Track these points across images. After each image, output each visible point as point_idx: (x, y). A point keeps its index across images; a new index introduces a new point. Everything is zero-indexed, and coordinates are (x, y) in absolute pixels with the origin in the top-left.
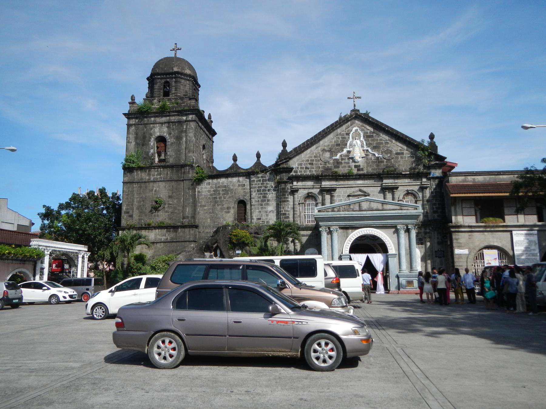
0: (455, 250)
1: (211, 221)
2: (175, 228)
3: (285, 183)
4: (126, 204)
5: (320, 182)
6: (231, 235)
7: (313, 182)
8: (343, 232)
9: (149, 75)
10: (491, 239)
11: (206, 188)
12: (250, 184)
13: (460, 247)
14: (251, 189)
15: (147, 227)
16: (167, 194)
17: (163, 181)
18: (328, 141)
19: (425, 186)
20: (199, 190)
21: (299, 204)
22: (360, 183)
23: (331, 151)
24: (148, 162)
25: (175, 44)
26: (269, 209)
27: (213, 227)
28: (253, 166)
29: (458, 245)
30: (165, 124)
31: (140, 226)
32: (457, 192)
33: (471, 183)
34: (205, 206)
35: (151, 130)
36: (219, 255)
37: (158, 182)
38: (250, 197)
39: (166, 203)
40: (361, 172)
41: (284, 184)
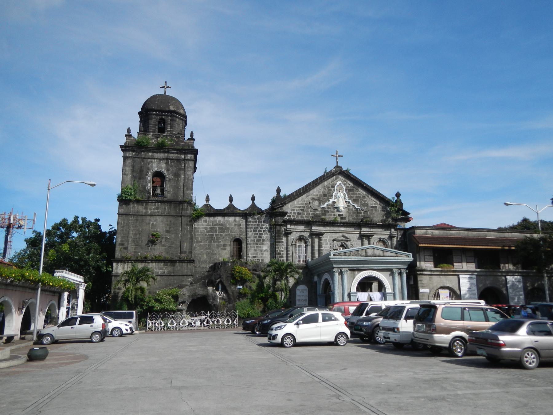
0: (420, 289)
1: (207, 257)
2: (172, 262)
3: (280, 225)
4: (121, 236)
5: (310, 226)
6: (233, 271)
7: (304, 227)
8: (351, 274)
9: (140, 110)
11: (203, 225)
12: (246, 224)
13: (423, 287)
14: (248, 229)
15: (143, 261)
16: (165, 228)
17: (161, 215)
18: (317, 191)
19: (394, 235)
20: (195, 226)
21: (292, 245)
22: (343, 230)
24: (145, 196)
25: (166, 82)
26: (264, 248)
27: (210, 262)
28: (250, 207)
29: (422, 285)
30: (163, 160)
31: (135, 258)
32: (428, 243)
33: (430, 236)
34: (201, 242)
35: (148, 165)
36: (220, 289)
37: (155, 217)
38: (245, 237)
39: (163, 237)
40: (344, 221)
41: (279, 227)
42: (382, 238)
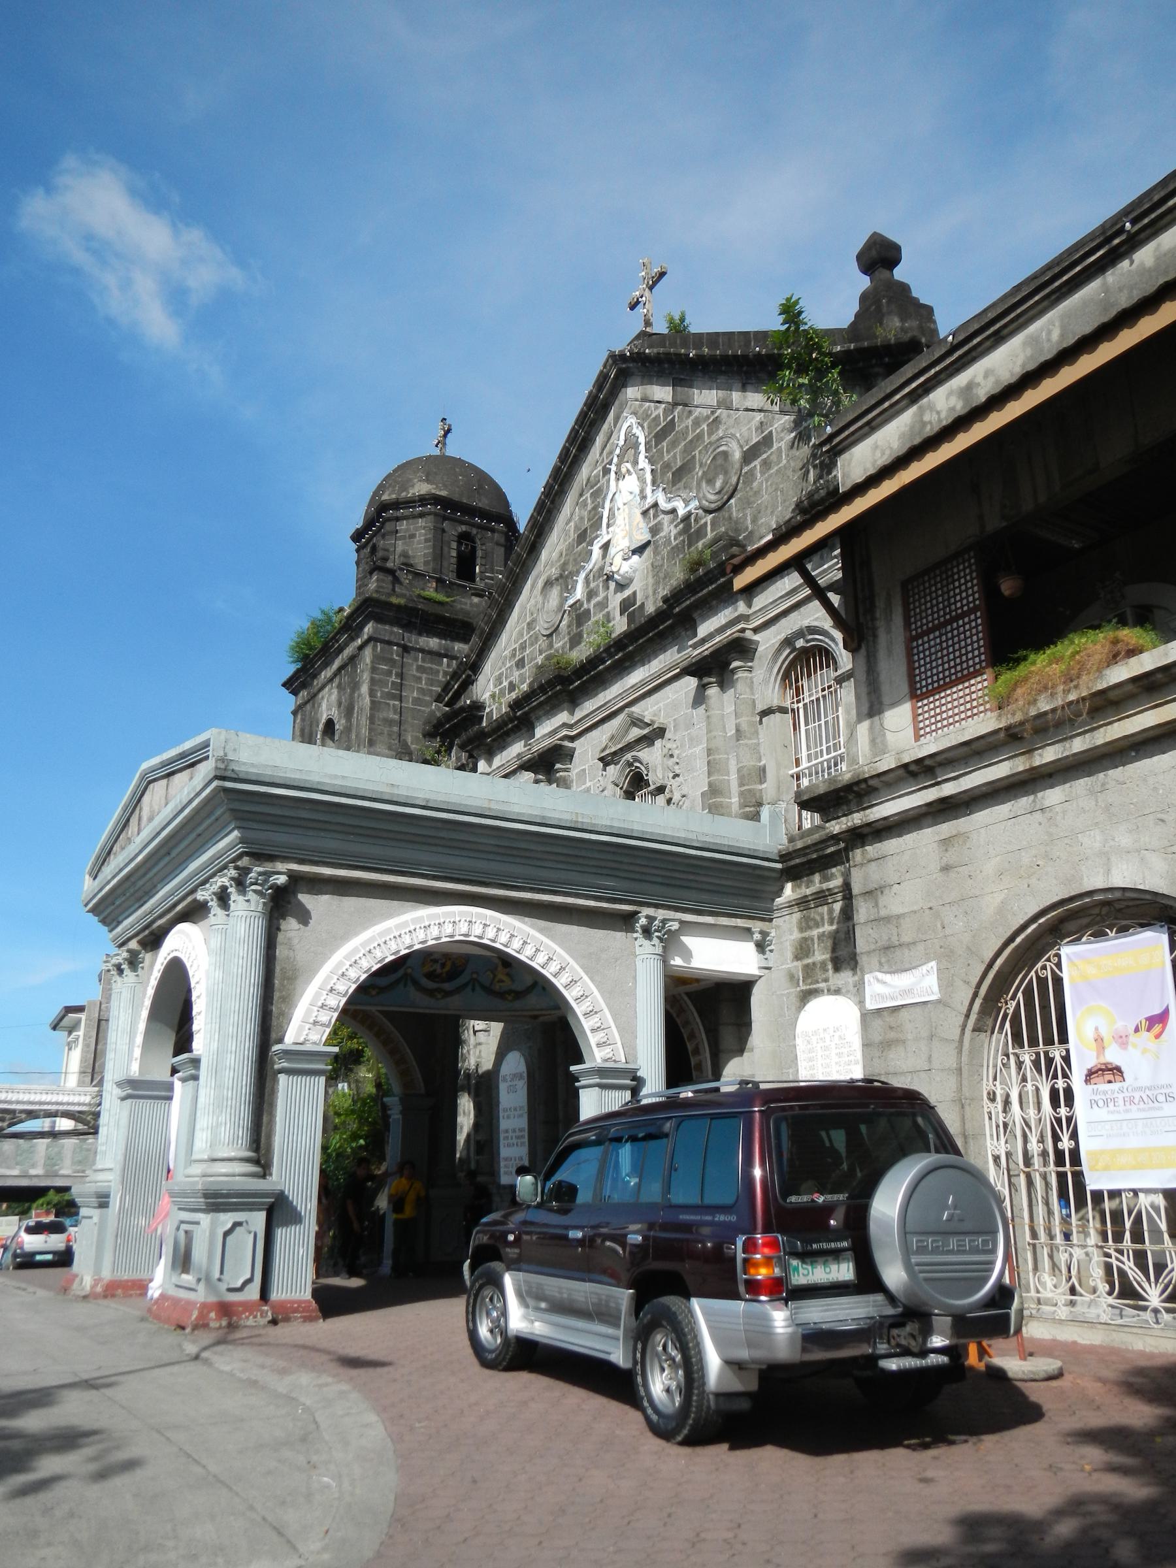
10: (1093, 841)
23: (561, 576)
29: (883, 934)
42: (800, 634)
